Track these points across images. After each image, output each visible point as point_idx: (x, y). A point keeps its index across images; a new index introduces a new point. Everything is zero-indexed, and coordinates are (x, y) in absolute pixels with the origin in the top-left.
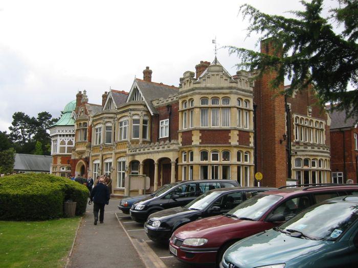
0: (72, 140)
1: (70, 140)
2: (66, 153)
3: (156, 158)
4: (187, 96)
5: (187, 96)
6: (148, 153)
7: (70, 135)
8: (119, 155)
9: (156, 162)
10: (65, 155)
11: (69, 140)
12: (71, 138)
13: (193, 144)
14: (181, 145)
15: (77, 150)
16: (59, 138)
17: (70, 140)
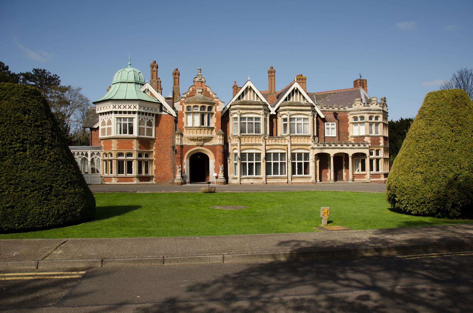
0: (151, 121)
1: (150, 120)
2: (145, 136)
3: (350, 152)
4: (375, 114)
5: (375, 114)
6: (342, 148)
7: (150, 114)
8: (293, 147)
9: (350, 155)
10: (143, 138)
11: (148, 120)
12: (150, 118)
13: (380, 145)
14: (370, 145)
15: (187, 134)
16: (136, 116)
17: (150, 120)
